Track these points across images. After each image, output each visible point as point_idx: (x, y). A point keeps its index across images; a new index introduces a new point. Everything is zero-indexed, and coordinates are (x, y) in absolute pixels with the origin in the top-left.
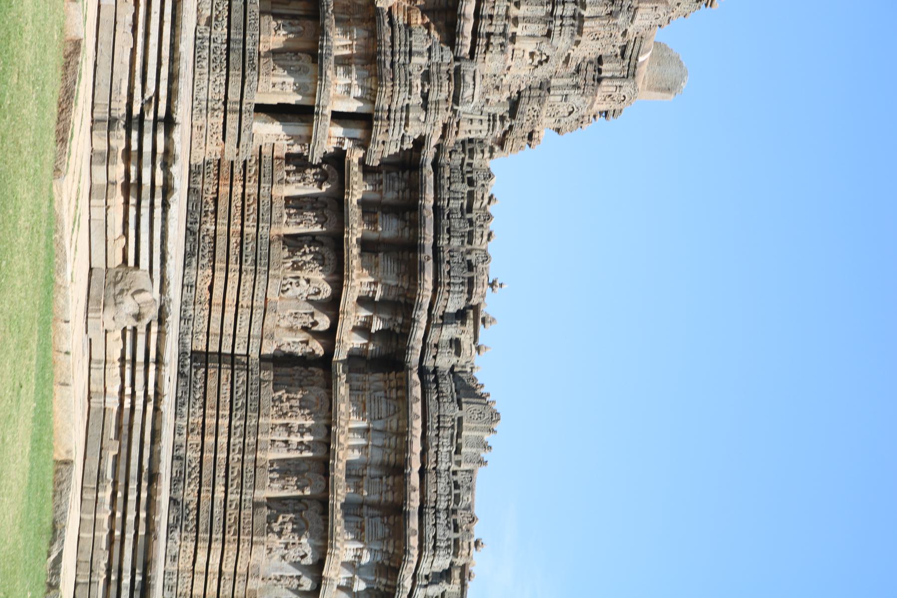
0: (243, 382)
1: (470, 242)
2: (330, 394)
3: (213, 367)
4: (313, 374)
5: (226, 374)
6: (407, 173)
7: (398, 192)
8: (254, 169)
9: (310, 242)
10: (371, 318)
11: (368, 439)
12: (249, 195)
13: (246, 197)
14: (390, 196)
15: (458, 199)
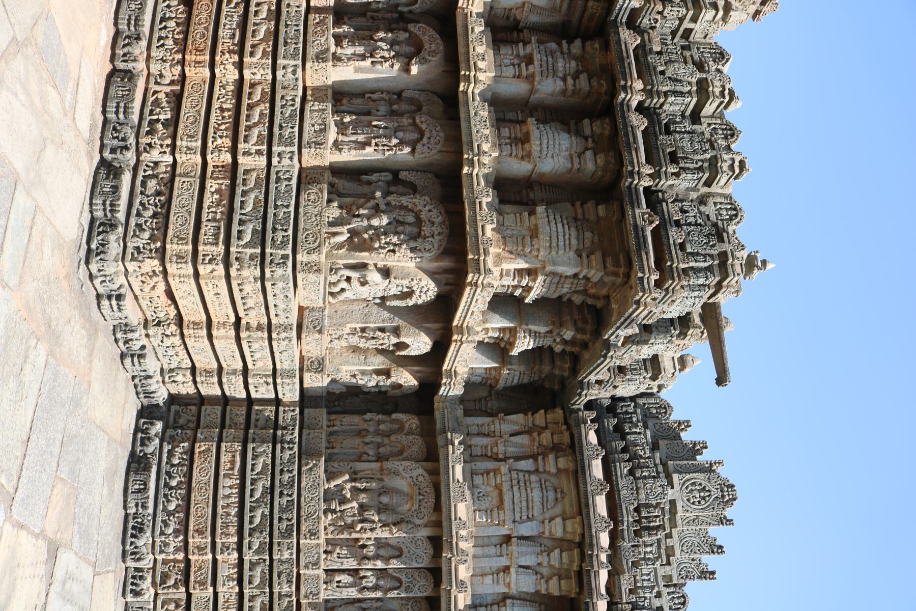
0: (265, 465)
1: (708, 184)
2: (435, 473)
3: (206, 439)
4: (401, 424)
5: (230, 452)
6: (578, 43)
7: (564, 80)
8: (263, 29)
9: (389, 183)
10: (513, 331)
11: (510, 556)
12: (253, 85)
13: (246, 89)
14: (548, 88)
15: (681, 94)
